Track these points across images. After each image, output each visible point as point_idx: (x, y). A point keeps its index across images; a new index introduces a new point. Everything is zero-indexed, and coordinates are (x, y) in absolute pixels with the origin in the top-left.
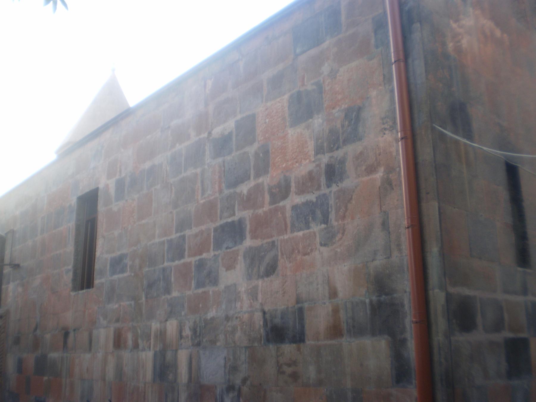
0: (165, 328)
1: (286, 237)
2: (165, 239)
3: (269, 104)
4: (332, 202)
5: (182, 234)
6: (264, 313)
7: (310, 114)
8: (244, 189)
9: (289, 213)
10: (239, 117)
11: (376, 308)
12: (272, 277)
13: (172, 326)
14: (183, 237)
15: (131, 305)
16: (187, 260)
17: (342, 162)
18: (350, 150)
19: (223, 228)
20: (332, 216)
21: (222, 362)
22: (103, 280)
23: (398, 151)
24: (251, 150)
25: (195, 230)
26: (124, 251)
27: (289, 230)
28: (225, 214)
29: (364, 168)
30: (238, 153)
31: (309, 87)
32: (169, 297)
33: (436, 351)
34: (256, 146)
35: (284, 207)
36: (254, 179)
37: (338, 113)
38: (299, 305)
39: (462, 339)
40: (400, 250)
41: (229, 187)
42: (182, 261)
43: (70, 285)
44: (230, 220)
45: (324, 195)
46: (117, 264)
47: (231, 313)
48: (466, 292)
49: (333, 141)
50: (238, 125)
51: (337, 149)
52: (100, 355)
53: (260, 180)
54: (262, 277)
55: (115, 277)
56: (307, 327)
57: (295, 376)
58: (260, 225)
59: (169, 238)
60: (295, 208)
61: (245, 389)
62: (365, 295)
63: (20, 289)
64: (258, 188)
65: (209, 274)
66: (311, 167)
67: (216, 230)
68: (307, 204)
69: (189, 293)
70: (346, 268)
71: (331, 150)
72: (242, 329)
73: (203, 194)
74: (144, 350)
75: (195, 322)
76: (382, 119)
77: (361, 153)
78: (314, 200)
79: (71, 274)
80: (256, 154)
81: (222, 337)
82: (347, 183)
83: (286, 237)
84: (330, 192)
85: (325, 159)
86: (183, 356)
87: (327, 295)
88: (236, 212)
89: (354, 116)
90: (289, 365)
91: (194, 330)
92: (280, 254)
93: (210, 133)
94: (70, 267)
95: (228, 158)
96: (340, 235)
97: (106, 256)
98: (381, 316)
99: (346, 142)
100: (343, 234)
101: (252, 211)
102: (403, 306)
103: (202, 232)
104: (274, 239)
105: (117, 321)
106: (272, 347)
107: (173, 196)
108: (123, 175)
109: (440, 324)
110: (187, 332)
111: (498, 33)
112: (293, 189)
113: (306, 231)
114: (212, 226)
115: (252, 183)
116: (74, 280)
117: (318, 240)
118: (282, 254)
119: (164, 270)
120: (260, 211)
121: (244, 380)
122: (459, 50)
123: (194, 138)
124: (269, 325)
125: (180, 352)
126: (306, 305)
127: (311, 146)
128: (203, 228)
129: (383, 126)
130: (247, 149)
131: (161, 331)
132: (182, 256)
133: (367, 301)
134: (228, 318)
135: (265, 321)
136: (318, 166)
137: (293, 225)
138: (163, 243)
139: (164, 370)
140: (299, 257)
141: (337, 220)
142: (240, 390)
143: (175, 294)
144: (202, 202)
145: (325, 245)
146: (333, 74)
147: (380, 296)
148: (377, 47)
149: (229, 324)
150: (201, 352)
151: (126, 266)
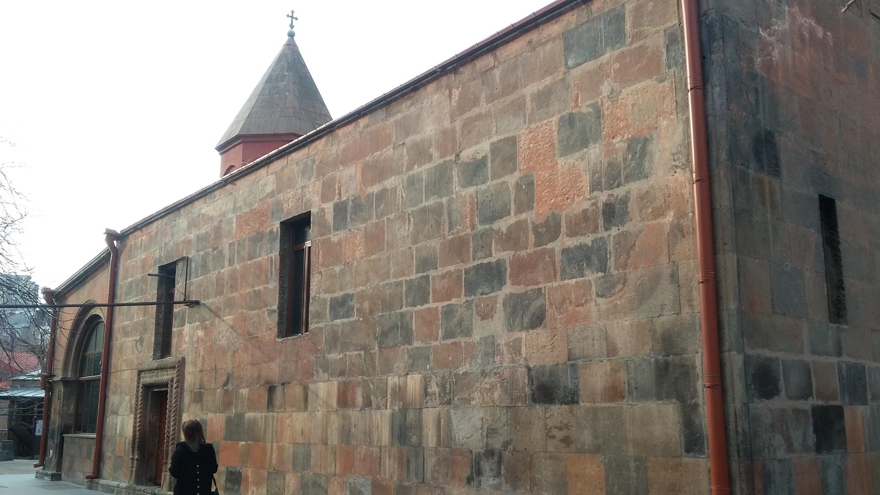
0: (406, 383)
1: (555, 284)
3: (533, 126)
4: (611, 247)
5: (425, 274)
6: (529, 369)
7: (585, 143)
8: (502, 225)
9: (558, 257)
10: (495, 139)
11: (663, 370)
12: (539, 330)
13: (414, 382)
14: (427, 277)
15: (360, 355)
16: (431, 305)
17: (625, 201)
18: (635, 188)
19: (477, 268)
20: (611, 263)
21: (479, 424)
22: (321, 325)
23: (691, 193)
24: (511, 180)
25: (441, 271)
26: (350, 291)
27: (558, 277)
28: (479, 254)
29: (650, 210)
30: (495, 182)
31: (584, 110)
32: (410, 347)
33: (732, 419)
34: (517, 175)
35: (553, 249)
36: (515, 215)
37: (619, 143)
38: (572, 362)
39: (763, 407)
40: (691, 306)
41: (483, 222)
42: (426, 306)
43: (276, 330)
44: (485, 261)
45: (601, 238)
46: (340, 306)
47: (488, 368)
48: (767, 353)
49: (611, 176)
50: (495, 149)
51: (618, 186)
52: (319, 414)
53: (523, 216)
54: (527, 329)
55: (338, 321)
56: (581, 386)
57: (567, 441)
58: (523, 268)
59: (408, 279)
60: (565, 251)
61: (507, 455)
62: (648, 351)
63: (200, 333)
64: (520, 224)
65: (461, 322)
66: (586, 205)
67: (467, 272)
68: (580, 247)
69: (434, 343)
71: (610, 187)
72: (502, 386)
73: (450, 229)
74: (378, 408)
75: (443, 377)
76: (673, 154)
77: (647, 193)
78: (590, 244)
79: (276, 316)
80: (518, 186)
81: (476, 395)
82: (628, 227)
83: (555, 284)
84: (609, 235)
85: (603, 197)
86: (429, 416)
87: (605, 352)
88: (493, 252)
89: (639, 148)
90: (561, 429)
92: (547, 303)
93: (458, 156)
94: (275, 307)
95: (483, 187)
96: (620, 286)
97: (323, 296)
98: (669, 377)
99: (629, 178)
100: (624, 284)
101: (513, 252)
102: (694, 367)
103: (449, 274)
104: (540, 286)
105: (342, 373)
106: (539, 408)
107: (412, 228)
108: (344, 199)
110: (434, 388)
111: (820, 33)
112: (563, 229)
113: (579, 279)
115: (512, 219)
116: (280, 323)
117: (594, 289)
118: (551, 304)
119: (402, 315)
120: (523, 253)
121: (506, 445)
122: (769, 66)
123: (437, 161)
126: (580, 362)
127: (586, 181)
128: (452, 268)
129: (674, 163)
130: (506, 178)
131: (400, 387)
132: (426, 301)
133: (652, 360)
135: (531, 379)
137: (563, 271)
138: (399, 284)
139: (404, 432)
140: (571, 308)
141: (616, 269)
142: (500, 457)
144: (450, 237)
145: (602, 296)
146: (613, 96)
147: (668, 356)
148: (669, 68)
149: (486, 380)
150: (452, 411)
151: (353, 309)
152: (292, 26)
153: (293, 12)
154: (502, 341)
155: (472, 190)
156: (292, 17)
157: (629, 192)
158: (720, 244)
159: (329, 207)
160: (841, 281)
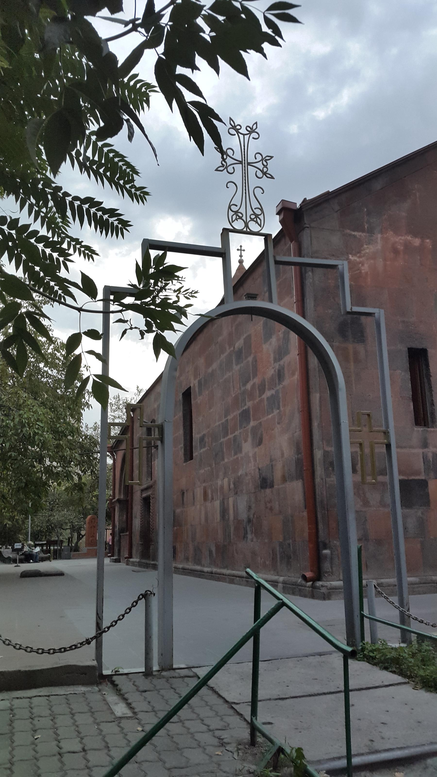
2: (220, 422)
6: (259, 470)
28: (243, 405)
43: (183, 458)
54: (258, 446)
70: (286, 438)
91: (234, 484)
93: (234, 347)
94: (182, 445)
109: (319, 471)
113: (272, 415)
114: (239, 412)
124: (261, 477)
125: (229, 499)
134: (246, 474)
135: (260, 474)
136: (275, 371)
138: (219, 425)
143: (226, 460)
147: (298, 455)
152: (241, 256)
153: (241, 246)
154: (251, 455)
155: (239, 367)
156: (241, 250)
157: (284, 363)
159: (196, 382)
160: (432, 400)
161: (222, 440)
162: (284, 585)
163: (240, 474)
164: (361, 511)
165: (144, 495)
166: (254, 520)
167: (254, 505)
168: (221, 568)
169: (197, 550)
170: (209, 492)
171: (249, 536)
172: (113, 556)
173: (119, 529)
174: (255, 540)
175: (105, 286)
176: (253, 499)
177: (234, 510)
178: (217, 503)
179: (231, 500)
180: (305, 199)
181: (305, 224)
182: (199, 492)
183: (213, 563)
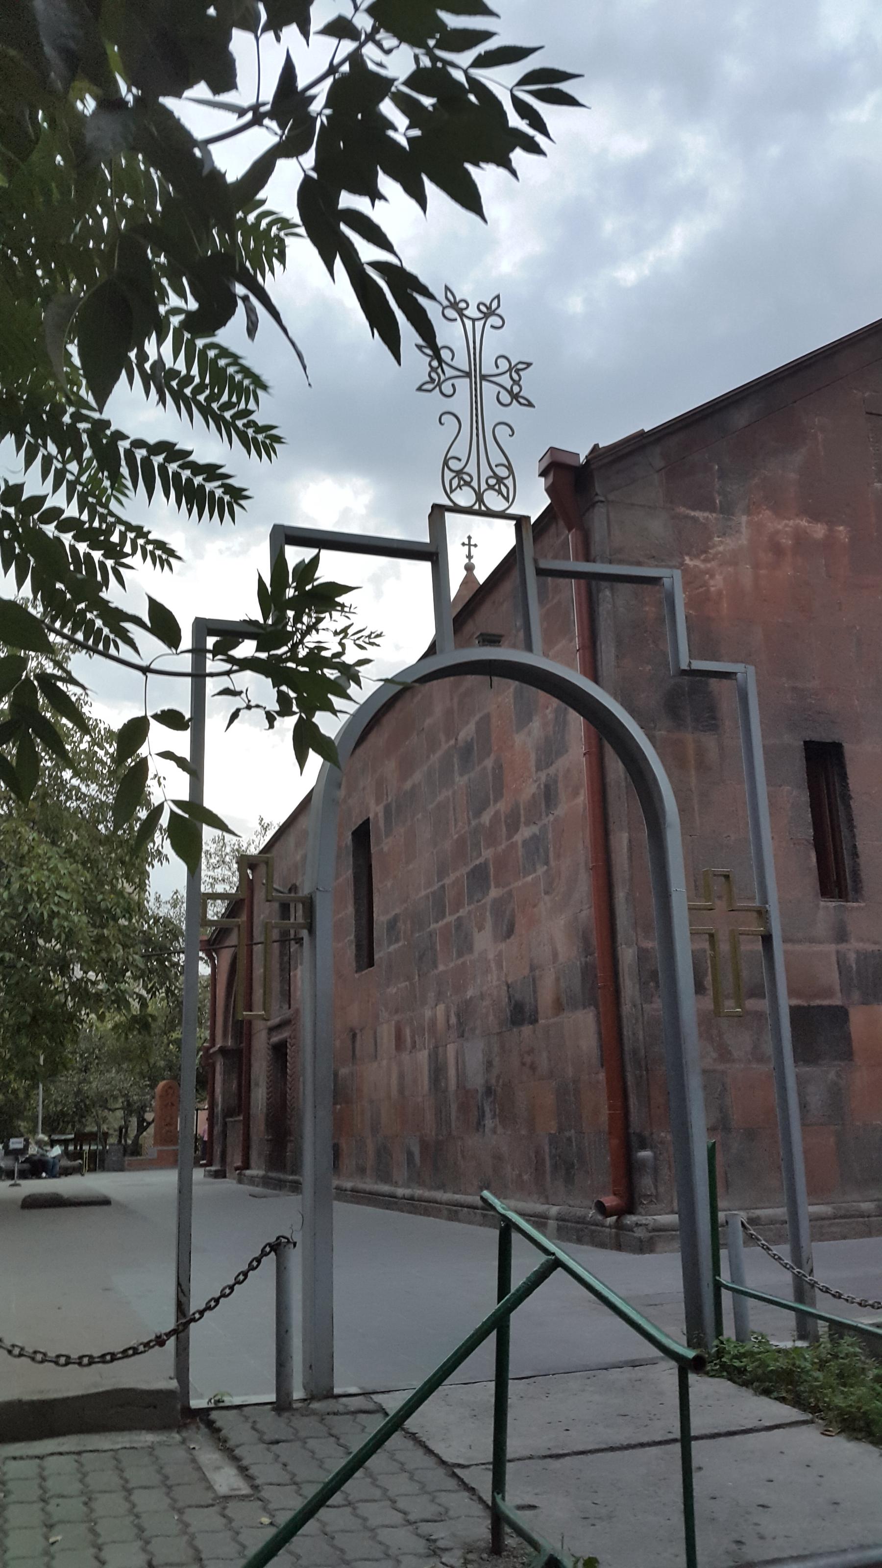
2: (429, 891)
6: (508, 987)
43: (354, 964)
52: (384, 1062)
70: (562, 922)
91: (458, 1016)
93: (456, 739)
94: (352, 937)
104: (512, 886)
109: (629, 988)
113: (534, 875)
124: (513, 1002)
134: (482, 997)
136: (539, 786)
138: (427, 897)
143: (441, 968)
147: (586, 957)
152: (469, 557)
153: (469, 538)
154: (491, 956)
155: (466, 778)
157: (558, 771)
158: (612, 827)
159: (380, 809)
160: (855, 846)
161: (432, 926)
162: (560, 1223)
163: (470, 993)
164: (714, 1071)
165: (275, 1039)
166: (499, 1090)
167: (497, 1059)
168: (431, 1188)
169: (383, 1153)
170: (408, 1032)
171: (489, 1123)
172: (210, 1164)
173: (223, 1110)
174: (500, 1130)
175: (196, 618)
176: (496, 1049)
177: (457, 1069)
178: (423, 1056)
179: (451, 1049)
180: (596, 446)
181: (597, 494)
182: (386, 1032)
183: (415, 1178)
